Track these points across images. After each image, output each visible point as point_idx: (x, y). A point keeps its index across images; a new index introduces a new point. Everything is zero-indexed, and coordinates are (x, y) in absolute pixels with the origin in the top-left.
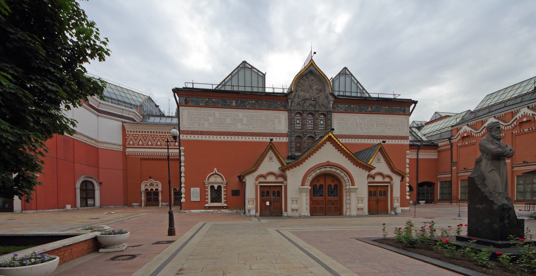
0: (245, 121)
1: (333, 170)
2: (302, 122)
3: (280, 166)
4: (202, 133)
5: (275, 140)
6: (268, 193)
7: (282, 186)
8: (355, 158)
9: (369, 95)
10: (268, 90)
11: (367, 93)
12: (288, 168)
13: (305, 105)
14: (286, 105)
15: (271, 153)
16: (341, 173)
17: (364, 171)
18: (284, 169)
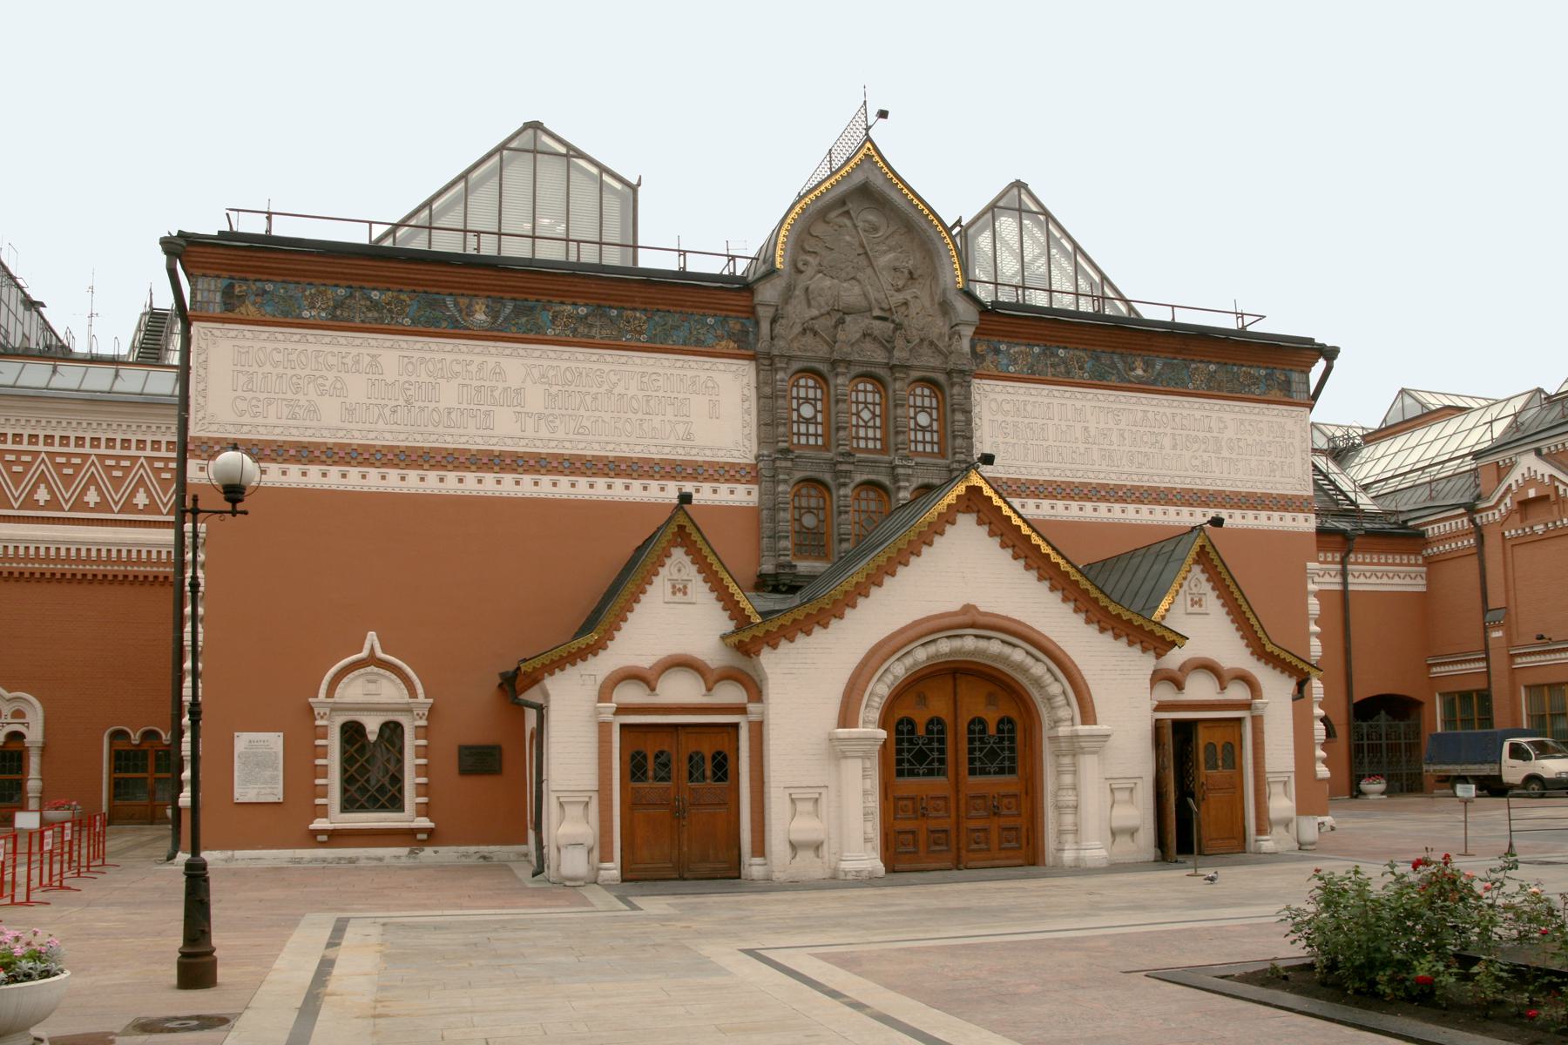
0: (535, 399)
1: (995, 647)
2: (827, 412)
3: (730, 626)
4: (305, 453)
6: (664, 765)
7: (736, 726)
8: (1095, 593)
9: (1131, 309)
10: (646, 261)
12: (771, 640)
13: (841, 336)
15: (678, 565)
16: (1029, 661)
18: (748, 641)
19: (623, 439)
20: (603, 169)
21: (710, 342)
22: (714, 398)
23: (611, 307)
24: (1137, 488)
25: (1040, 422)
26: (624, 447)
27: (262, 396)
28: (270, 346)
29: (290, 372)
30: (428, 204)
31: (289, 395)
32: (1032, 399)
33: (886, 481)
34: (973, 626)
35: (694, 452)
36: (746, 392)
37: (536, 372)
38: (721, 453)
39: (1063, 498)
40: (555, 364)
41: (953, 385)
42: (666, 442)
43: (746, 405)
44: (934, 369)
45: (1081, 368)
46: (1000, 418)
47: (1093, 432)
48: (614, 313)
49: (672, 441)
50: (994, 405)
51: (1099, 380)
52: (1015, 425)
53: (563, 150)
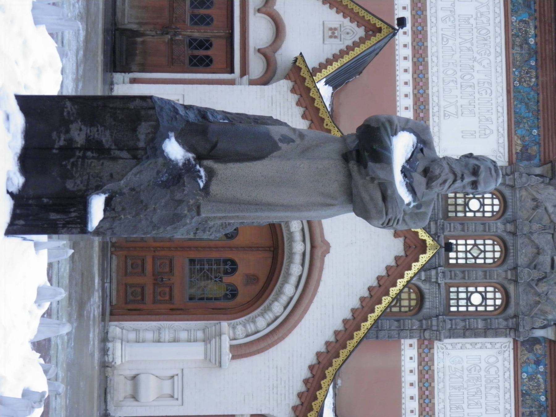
5: (403, 39)
7: (232, 71)
14: (530, 158)
16: (284, 299)
21: (519, 132)
22: (477, 135)
25: (483, 401)
26: (435, 69)
32: (501, 394)
34: (313, 247)
35: (436, 119)
37: (484, 9)
40: (492, 22)
41: (506, 320)
44: (517, 304)
48: (533, 63)
49: (443, 103)
50: (492, 360)
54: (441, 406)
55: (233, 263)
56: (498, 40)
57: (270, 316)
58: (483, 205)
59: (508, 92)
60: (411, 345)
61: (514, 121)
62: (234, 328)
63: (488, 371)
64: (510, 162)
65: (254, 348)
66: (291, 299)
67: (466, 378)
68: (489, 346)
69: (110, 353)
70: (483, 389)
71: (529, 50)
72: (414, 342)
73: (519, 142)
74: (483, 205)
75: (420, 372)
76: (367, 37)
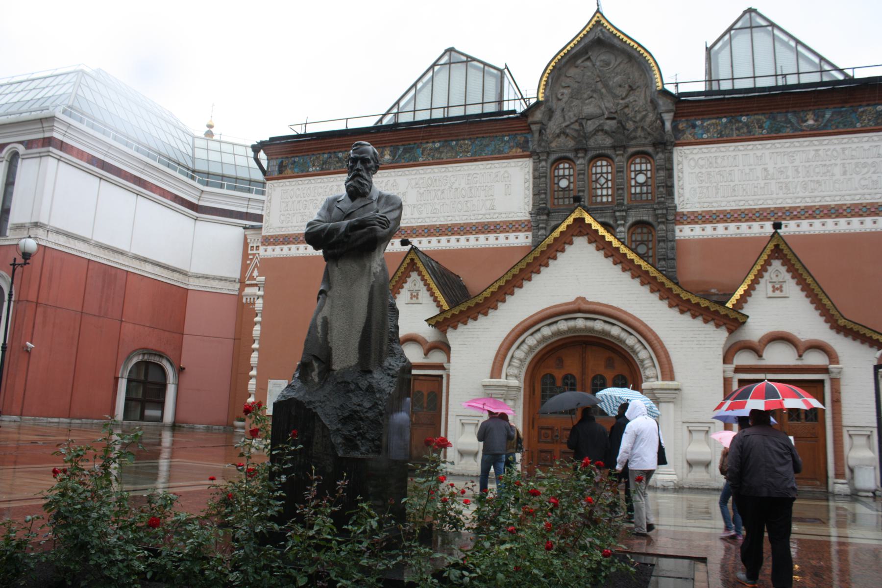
11: (836, 69)
16: (624, 335)
17: (711, 327)
19: (457, 213)
20: (485, 64)
21: (506, 151)
22: (508, 183)
23: (452, 140)
24: (811, 207)
25: (728, 169)
26: (457, 218)
27: (291, 213)
28: (296, 187)
29: (303, 199)
30: (398, 103)
31: (302, 211)
32: (722, 154)
33: (611, 222)
34: (579, 311)
35: (495, 216)
36: (527, 177)
37: (413, 183)
38: (511, 215)
39: (747, 221)
41: (657, 153)
42: (480, 212)
43: (527, 184)
45: (761, 127)
46: (697, 170)
47: (771, 170)
48: (454, 143)
49: (484, 211)
50: (692, 163)
51: (776, 134)
52: (709, 174)
53: (464, 59)
54: (733, 204)
55: (595, 378)
56: (436, 170)
57: (638, 347)
58: (564, 177)
59: (476, 160)
60: (681, 231)
61: (500, 155)
62: (648, 378)
63: (702, 166)
64: (529, 156)
65: (664, 360)
66: (623, 329)
67: (708, 185)
68: (680, 166)
69: (666, 485)
70: (717, 170)
71: (443, 146)
72: (677, 228)
73: (514, 150)
74: (564, 177)
75: (704, 222)
76: (417, 269)
